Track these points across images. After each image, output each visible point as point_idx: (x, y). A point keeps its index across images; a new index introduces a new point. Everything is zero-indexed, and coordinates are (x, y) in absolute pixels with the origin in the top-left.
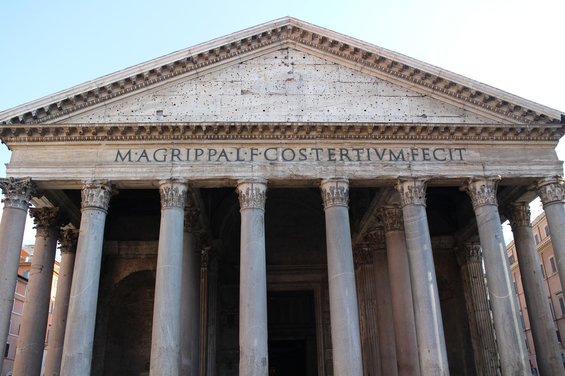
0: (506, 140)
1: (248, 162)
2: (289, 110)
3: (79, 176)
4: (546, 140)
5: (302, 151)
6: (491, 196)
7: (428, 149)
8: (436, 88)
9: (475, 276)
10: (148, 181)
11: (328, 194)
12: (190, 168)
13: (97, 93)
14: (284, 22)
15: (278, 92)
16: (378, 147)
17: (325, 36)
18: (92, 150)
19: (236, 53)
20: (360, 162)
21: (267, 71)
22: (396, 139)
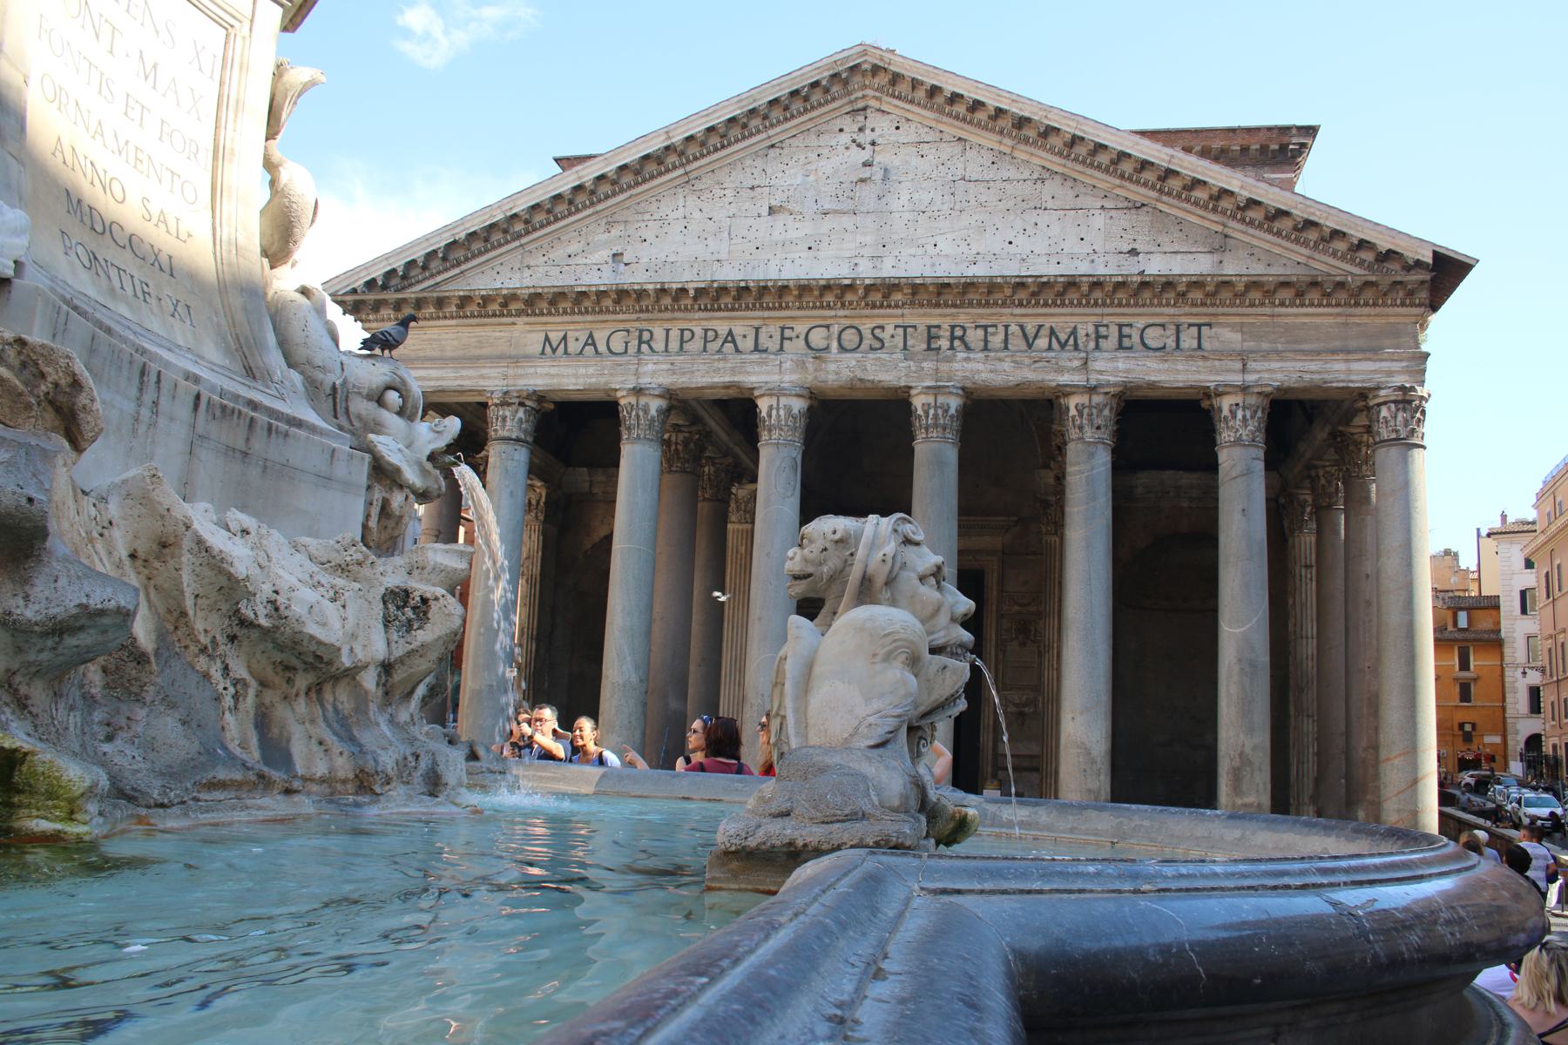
0: (1302, 305)
1: (776, 355)
2: (858, 244)
3: (482, 383)
4: (1396, 305)
5: (877, 331)
6: (1249, 428)
7: (1130, 325)
8: (1166, 189)
9: (1308, 563)
10: (595, 390)
11: (920, 416)
12: (669, 366)
13: (505, 226)
15: (838, 208)
17: (935, 83)
18: (503, 334)
20: (986, 353)
21: (823, 162)
22: (1063, 305)
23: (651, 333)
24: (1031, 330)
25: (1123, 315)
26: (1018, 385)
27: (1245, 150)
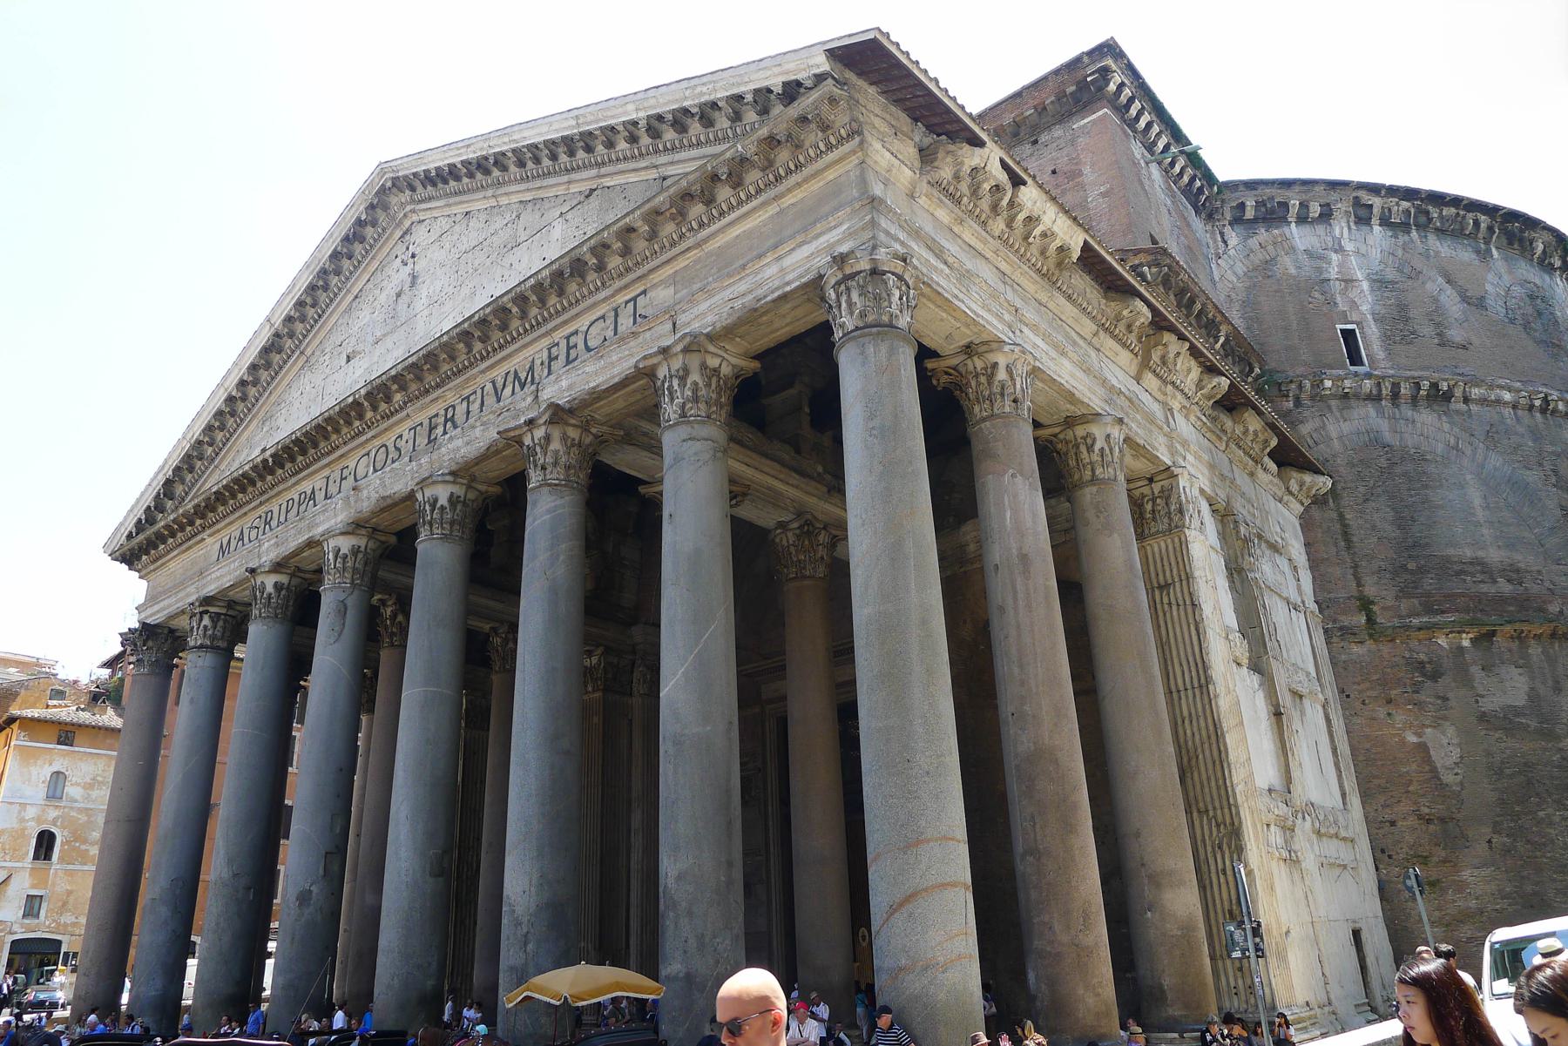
0: (722, 214)
6: (676, 401)
7: (576, 332)
9: (1162, 583)
14: (377, 180)
23: (271, 511)
25: (565, 323)
26: (488, 449)
27: (1041, 110)
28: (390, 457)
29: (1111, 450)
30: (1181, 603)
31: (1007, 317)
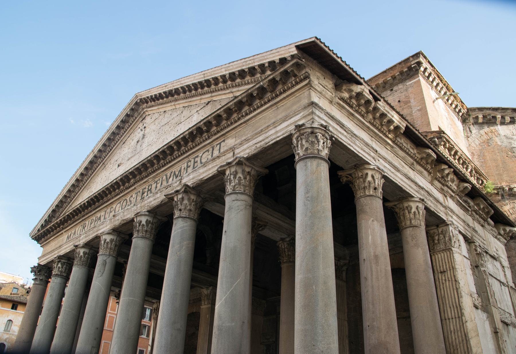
6: (232, 184)
9: (442, 270)
14: (135, 99)
16: (167, 172)
19: (118, 138)
22: (174, 159)
23: (86, 223)
24: (169, 175)
25: (194, 152)
26: (162, 202)
27: (394, 78)
28: (128, 204)
29: (419, 213)
30: (450, 280)
31: (372, 154)
